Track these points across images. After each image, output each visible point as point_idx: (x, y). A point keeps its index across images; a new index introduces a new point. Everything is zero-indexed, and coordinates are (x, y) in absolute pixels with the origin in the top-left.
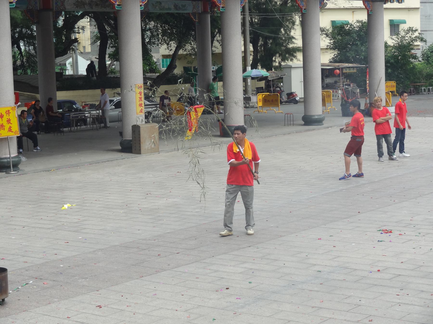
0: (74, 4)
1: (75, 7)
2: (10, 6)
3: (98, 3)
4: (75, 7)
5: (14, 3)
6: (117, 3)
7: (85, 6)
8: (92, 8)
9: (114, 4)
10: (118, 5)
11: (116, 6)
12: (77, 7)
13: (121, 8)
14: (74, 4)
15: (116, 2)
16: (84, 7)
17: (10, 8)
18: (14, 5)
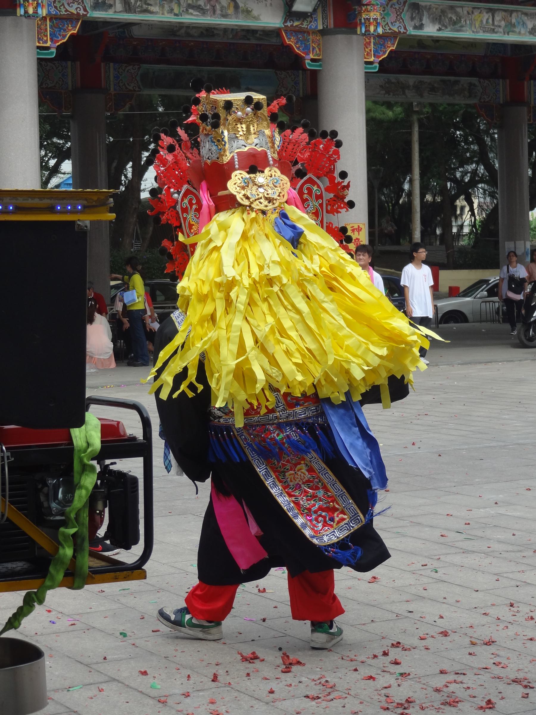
0: (381, 86)
1: (384, 92)
2: (38, 54)
3: (436, 85)
4: (384, 92)
5: (54, 50)
6: (311, 56)
7: (407, 91)
8: (421, 96)
9: (303, 59)
10: (313, 60)
11: (307, 61)
12: (388, 92)
13: (320, 66)
14: (381, 86)
15: (307, 54)
16: (404, 93)
17: (38, 59)
18: (52, 53)
